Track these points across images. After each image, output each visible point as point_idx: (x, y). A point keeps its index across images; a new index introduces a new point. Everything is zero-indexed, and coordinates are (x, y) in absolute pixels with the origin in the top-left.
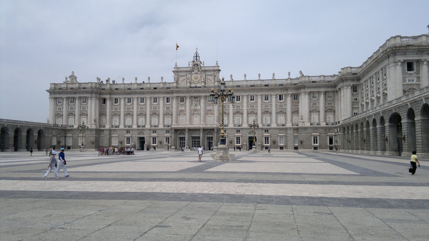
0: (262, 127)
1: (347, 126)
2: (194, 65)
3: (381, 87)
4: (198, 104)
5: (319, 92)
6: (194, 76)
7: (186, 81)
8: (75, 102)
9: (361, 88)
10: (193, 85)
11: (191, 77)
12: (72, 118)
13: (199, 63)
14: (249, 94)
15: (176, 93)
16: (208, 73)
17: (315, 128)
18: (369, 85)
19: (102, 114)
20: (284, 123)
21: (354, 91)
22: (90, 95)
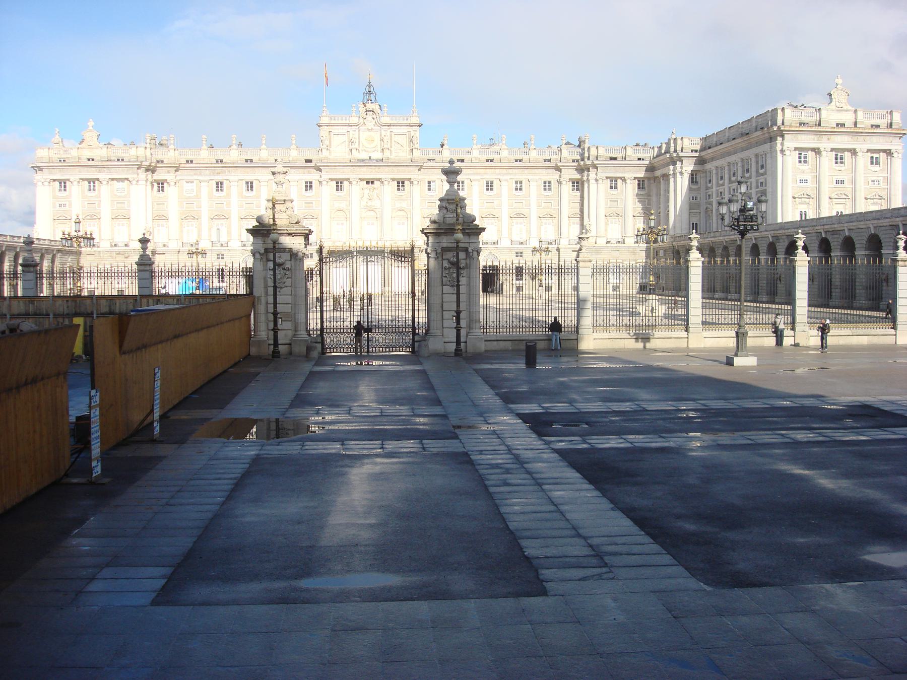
0: (511, 246)
1: (684, 249)
2: (367, 111)
3: (754, 185)
4: (376, 196)
5: (623, 179)
6: (364, 135)
7: (348, 145)
8: (99, 190)
9: (706, 177)
10: (365, 156)
11: (359, 139)
12: (94, 225)
13: (376, 107)
14: (484, 177)
15: (327, 172)
16: (395, 130)
17: (615, 250)
18: (726, 176)
19: (160, 217)
20: (554, 239)
21: (692, 182)
22: (136, 175)
